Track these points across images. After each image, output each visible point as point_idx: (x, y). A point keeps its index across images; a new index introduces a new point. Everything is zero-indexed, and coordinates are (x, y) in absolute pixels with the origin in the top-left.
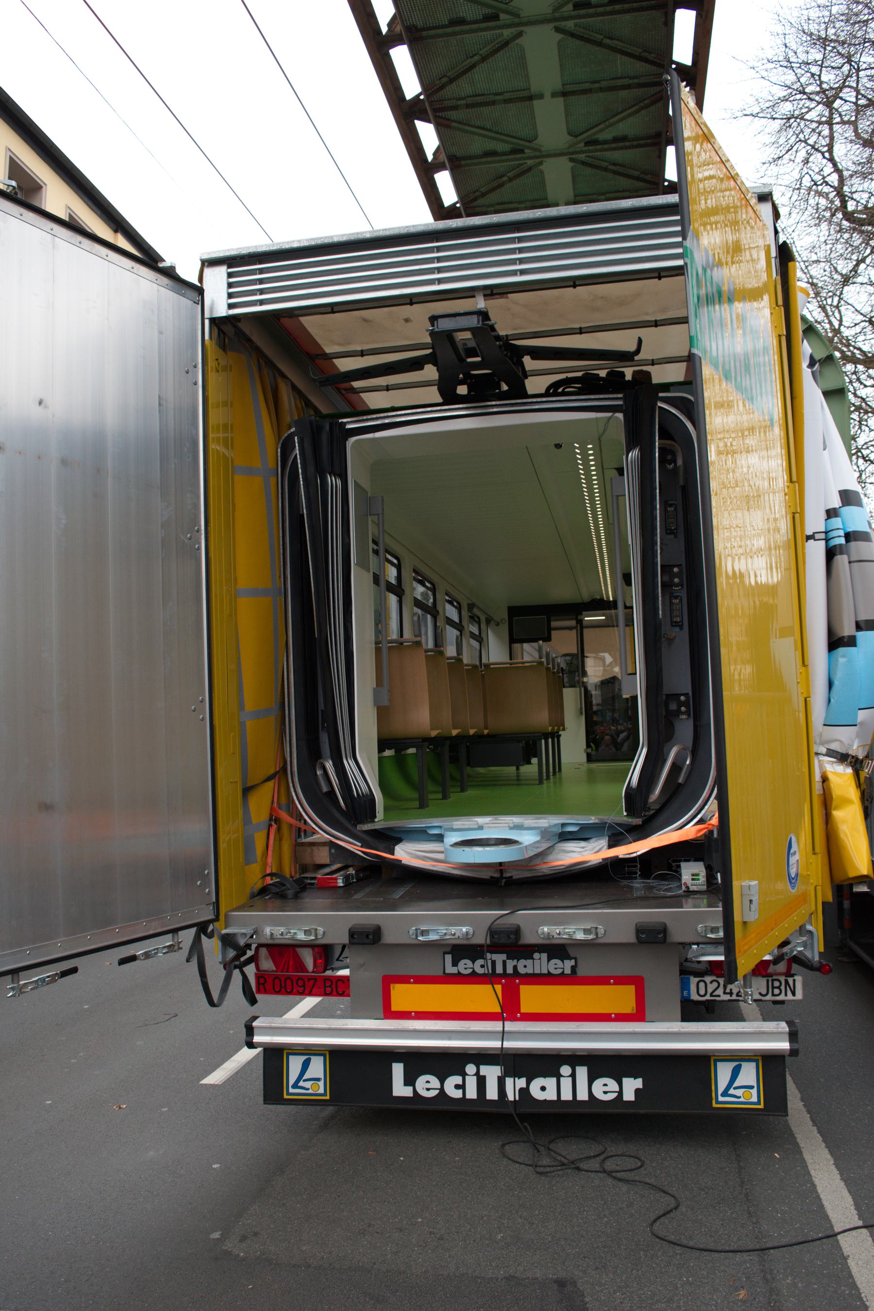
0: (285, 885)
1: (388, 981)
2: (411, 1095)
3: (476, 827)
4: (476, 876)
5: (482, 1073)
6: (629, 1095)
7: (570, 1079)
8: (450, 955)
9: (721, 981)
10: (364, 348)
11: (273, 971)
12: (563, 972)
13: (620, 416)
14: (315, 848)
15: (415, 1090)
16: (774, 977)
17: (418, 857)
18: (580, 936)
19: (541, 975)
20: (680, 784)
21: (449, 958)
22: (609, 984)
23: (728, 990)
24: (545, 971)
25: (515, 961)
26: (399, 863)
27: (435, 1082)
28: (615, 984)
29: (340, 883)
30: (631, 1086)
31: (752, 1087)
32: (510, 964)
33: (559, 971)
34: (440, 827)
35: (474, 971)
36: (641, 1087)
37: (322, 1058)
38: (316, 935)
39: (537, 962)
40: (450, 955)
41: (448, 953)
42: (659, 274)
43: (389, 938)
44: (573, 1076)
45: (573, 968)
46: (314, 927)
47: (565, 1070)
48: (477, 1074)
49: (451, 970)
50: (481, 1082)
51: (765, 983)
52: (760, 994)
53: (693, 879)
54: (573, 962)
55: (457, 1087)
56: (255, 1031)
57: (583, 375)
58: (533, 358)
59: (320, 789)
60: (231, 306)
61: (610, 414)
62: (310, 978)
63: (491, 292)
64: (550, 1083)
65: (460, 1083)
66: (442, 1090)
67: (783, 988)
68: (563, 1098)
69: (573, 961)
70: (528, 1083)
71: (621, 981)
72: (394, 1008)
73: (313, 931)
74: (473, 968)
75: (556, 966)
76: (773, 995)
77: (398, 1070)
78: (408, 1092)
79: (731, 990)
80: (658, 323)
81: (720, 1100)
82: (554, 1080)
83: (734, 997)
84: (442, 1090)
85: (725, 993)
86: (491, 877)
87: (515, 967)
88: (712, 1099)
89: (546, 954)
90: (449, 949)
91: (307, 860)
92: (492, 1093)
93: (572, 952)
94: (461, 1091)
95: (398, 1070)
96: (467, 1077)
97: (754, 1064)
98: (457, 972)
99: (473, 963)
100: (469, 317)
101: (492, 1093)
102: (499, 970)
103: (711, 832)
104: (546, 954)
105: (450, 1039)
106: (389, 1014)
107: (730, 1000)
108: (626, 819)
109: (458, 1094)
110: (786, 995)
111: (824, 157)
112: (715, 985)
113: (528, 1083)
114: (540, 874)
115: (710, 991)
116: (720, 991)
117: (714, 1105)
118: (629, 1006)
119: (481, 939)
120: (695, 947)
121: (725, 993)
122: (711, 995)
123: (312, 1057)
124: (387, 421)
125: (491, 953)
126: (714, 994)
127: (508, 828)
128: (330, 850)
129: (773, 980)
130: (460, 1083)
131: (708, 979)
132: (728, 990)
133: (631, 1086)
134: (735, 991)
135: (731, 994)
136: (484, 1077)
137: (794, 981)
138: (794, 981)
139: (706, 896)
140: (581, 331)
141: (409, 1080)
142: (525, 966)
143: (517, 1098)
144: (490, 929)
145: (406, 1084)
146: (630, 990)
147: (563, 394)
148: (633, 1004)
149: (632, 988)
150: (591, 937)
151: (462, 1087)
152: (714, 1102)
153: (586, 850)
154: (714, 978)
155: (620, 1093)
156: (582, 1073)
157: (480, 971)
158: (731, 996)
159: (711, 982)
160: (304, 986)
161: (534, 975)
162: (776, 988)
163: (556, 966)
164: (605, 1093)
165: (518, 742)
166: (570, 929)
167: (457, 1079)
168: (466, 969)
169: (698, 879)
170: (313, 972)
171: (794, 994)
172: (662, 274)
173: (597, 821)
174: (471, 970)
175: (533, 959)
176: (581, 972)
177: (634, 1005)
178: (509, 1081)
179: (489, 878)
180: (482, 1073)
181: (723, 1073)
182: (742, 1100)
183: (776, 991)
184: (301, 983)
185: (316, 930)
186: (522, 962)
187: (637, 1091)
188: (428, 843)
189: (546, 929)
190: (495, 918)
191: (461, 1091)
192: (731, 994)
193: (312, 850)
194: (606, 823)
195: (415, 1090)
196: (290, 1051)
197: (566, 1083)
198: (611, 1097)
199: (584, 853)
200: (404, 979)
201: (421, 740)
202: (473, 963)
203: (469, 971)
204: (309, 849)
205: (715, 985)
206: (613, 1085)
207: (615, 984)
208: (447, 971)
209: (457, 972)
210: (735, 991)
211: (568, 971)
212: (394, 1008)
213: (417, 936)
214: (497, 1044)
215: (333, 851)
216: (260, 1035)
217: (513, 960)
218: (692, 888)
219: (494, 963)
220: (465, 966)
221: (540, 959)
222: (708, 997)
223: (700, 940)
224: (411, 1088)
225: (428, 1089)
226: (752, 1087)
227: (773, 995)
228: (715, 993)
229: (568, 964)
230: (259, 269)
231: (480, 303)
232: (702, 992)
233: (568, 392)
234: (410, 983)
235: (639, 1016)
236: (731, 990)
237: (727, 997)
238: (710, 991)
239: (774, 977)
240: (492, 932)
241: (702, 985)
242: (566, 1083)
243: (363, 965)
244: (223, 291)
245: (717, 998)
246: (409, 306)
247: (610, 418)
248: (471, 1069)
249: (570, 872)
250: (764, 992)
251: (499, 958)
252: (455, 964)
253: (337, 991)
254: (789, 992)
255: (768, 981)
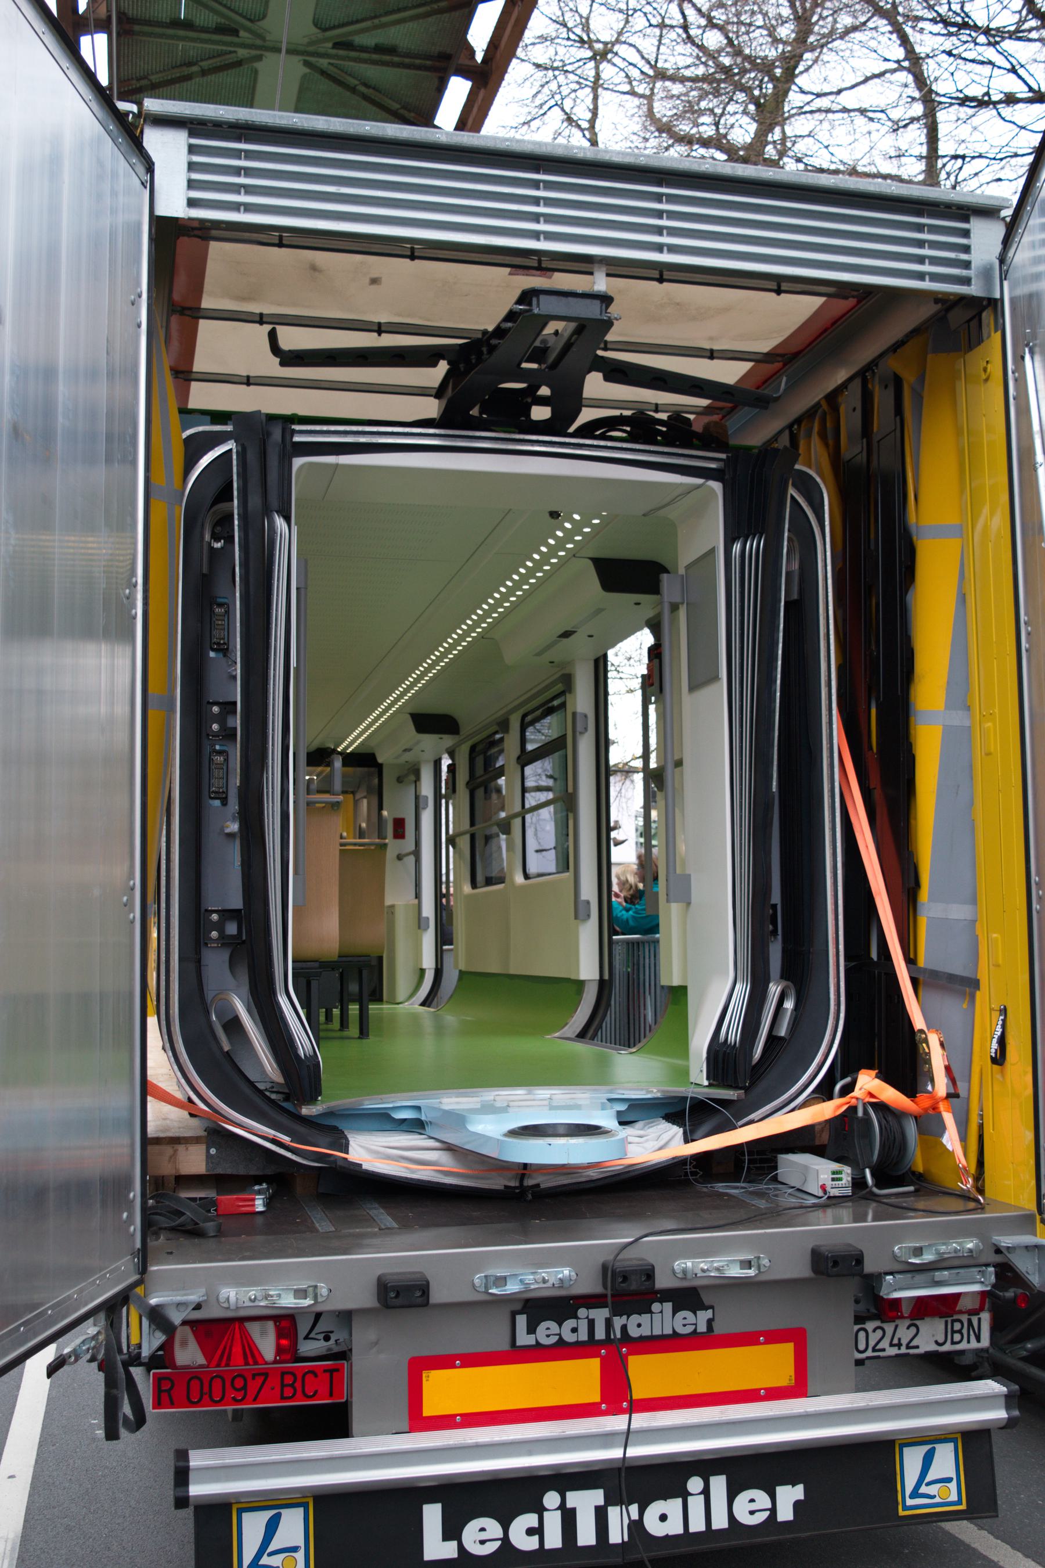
0: (184, 1214)
1: (418, 1367)
2: (455, 1555)
3: (479, 1106)
4: (486, 1186)
5: (569, 1504)
6: (785, 1514)
7: (702, 1496)
8: (524, 1317)
9: (889, 1328)
10: (265, 312)
11: (201, 1366)
12: (695, 1329)
13: (716, 486)
14: (181, 1148)
15: (461, 1547)
16: (955, 1317)
17: (389, 1158)
18: (735, 1272)
19: (663, 1337)
20: (781, 1038)
21: (522, 1321)
22: (758, 1343)
23: (895, 1341)
24: (668, 1331)
25: (625, 1317)
26: (357, 1168)
27: (494, 1528)
28: (767, 1342)
29: (259, 1205)
30: (789, 1496)
31: (950, 1480)
32: (618, 1322)
33: (689, 1329)
34: (418, 1108)
35: (561, 1339)
36: (802, 1497)
37: (301, 1510)
38: (315, 1297)
39: (657, 1317)
40: (524, 1317)
41: (520, 1313)
42: (661, 275)
43: (437, 1296)
44: (706, 1492)
45: (710, 1322)
46: (314, 1284)
47: (695, 1484)
48: (562, 1507)
49: (524, 1339)
50: (569, 1518)
51: (943, 1326)
52: (937, 1342)
53: (833, 1180)
54: (709, 1314)
55: (530, 1532)
56: (192, 1476)
57: (633, 414)
58: (607, 379)
59: (221, 1048)
60: (192, 203)
61: (699, 481)
62: (265, 1374)
63: (617, 268)
64: (673, 1507)
65: (536, 1525)
66: (505, 1540)
67: (965, 1331)
68: (693, 1529)
69: (710, 1311)
70: (641, 1513)
71: (774, 1337)
72: (427, 1412)
73: (311, 1289)
74: (560, 1335)
75: (685, 1322)
76: (953, 1343)
77: (432, 1515)
78: (448, 1551)
79: (899, 1339)
80: (715, 355)
81: (910, 1504)
82: (679, 1501)
83: (903, 1350)
84: (505, 1540)
85: (891, 1345)
86: (506, 1187)
87: (624, 1328)
88: (897, 1504)
89: (671, 1303)
90: (518, 1307)
91: (166, 1169)
92: (586, 1536)
93: (707, 1299)
94: (536, 1538)
95: (432, 1515)
96: (545, 1514)
97: (951, 1445)
98: (534, 1343)
99: (560, 1325)
100: (588, 301)
101: (586, 1536)
102: (600, 1334)
103: (853, 1109)
104: (671, 1303)
105: (530, 1453)
106: (419, 1422)
107: (897, 1355)
108: (706, 1090)
109: (531, 1544)
110: (969, 1342)
111: (584, 136)
112: (879, 1333)
113: (641, 1513)
114: (583, 1179)
115: (872, 1343)
116: (885, 1344)
117: (902, 1513)
118: (785, 1377)
119: (590, 1286)
120: (889, 1278)
121: (891, 1345)
122: (874, 1350)
123: (281, 1511)
124: (363, 440)
125: (588, 1308)
126: (878, 1347)
127: (548, 1108)
128: (208, 1151)
129: (953, 1321)
130: (536, 1525)
131: (870, 1326)
132: (895, 1341)
133: (789, 1496)
134: (904, 1342)
135: (899, 1345)
136: (573, 1510)
137: (979, 1319)
138: (979, 1319)
139: (850, 1204)
140: (712, 355)
141: (452, 1531)
142: (639, 1326)
143: (626, 1539)
144: (605, 1268)
145: (447, 1537)
146: (789, 1347)
147: (603, 437)
148: (791, 1371)
149: (789, 1347)
150: (751, 1272)
151: (537, 1531)
152: (900, 1507)
153: (647, 1141)
154: (877, 1323)
155: (773, 1510)
156: (719, 1484)
157: (569, 1338)
158: (899, 1349)
159: (874, 1331)
160: (244, 1388)
161: (652, 1339)
162: (957, 1332)
163: (685, 1322)
164: (752, 1513)
165: (333, 969)
166: (718, 1261)
167: (530, 1520)
168: (548, 1336)
169: (840, 1179)
170: (275, 1362)
171: (978, 1340)
172: (784, 286)
173: (659, 1095)
174: (555, 1339)
175: (651, 1312)
176: (719, 1329)
177: (792, 1373)
178: (614, 1513)
179: (502, 1188)
180: (569, 1504)
181: (912, 1461)
182: (937, 1500)
183: (957, 1337)
184: (239, 1383)
185: (316, 1287)
186: (635, 1319)
187: (797, 1505)
188: (381, 1133)
189: (689, 1264)
190: (616, 1252)
191: (536, 1538)
192: (899, 1345)
193: (176, 1151)
194: (685, 1098)
195: (461, 1547)
196: (244, 1505)
197: (696, 1504)
198: (761, 1517)
199: (645, 1145)
200: (445, 1362)
201: (317, 965)
202: (560, 1325)
203: (553, 1340)
204: (168, 1150)
205: (879, 1333)
206: (762, 1499)
207: (766, 1343)
208: (519, 1343)
209: (534, 1343)
210: (904, 1342)
211: (702, 1328)
212: (427, 1412)
213: (487, 1287)
214: (616, 1453)
215: (213, 1151)
216: (201, 1481)
217: (621, 1316)
218: (835, 1192)
219: (591, 1324)
220: (547, 1332)
221: (661, 1312)
222: (869, 1353)
223: (897, 1267)
224: (454, 1544)
225: (482, 1542)
226: (950, 1480)
227: (953, 1343)
228: (913, 1344)
229: (704, 1316)
230: (246, 151)
231: (601, 283)
232: (862, 1347)
233: (611, 436)
234: (454, 1367)
235: (798, 1389)
236: (899, 1339)
237: (893, 1351)
238: (872, 1343)
239: (955, 1317)
240: (607, 1271)
241: (862, 1335)
242: (696, 1504)
243: (376, 1343)
244: (181, 176)
245: (881, 1354)
246: (408, 260)
247: (699, 487)
248: (551, 1499)
249: (627, 1176)
250: (941, 1340)
251: (600, 1315)
252: (531, 1330)
253: (211, 1398)
254: (973, 1338)
255: (946, 1322)
